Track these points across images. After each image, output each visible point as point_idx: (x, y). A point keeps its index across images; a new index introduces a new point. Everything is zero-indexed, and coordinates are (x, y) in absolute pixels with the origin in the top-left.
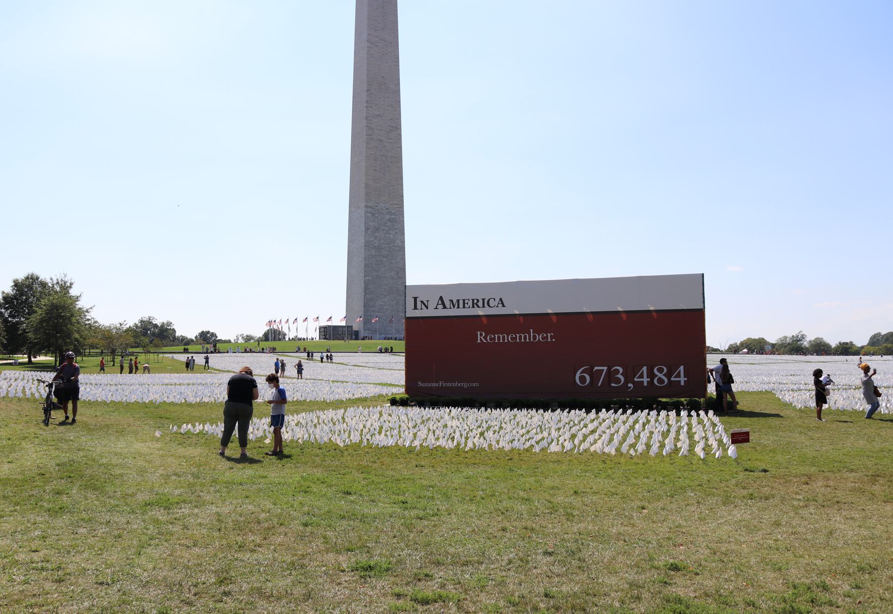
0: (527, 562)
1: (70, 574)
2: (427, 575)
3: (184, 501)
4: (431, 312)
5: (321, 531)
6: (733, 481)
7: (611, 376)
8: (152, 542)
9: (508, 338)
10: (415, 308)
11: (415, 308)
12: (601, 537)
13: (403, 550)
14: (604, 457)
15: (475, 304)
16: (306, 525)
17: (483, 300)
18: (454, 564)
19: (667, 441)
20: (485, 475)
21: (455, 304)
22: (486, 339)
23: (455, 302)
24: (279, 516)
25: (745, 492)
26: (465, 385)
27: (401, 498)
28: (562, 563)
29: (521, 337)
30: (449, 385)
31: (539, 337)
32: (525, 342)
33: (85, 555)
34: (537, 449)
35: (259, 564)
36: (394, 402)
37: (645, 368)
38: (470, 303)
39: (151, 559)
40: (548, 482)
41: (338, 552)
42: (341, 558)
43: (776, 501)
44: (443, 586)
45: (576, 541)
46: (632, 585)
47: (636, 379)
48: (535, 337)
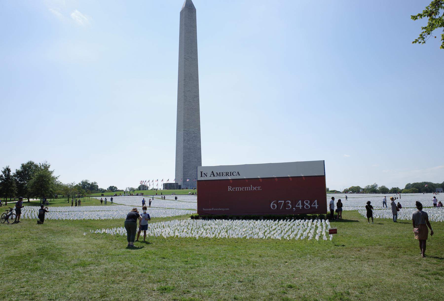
0: (231, 285)
1: (37, 296)
2: (188, 291)
3: (92, 264)
5: (149, 275)
6: (328, 250)
7: (286, 205)
8: (75, 281)
9: (242, 189)
10: (202, 176)
11: (202, 176)
12: (264, 275)
13: (181, 281)
14: (276, 241)
15: (227, 174)
16: (142, 272)
18: (201, 286)
19: (304, 233)
20: (224, 249)
24: (132, 269)
25: (331, 255)
26: (223, 210)
27: (186, 260)
28: (245, 285)
29: (247, 189)
30: (216, 209)
31: (255, 188)
33: (45, 288)
34: (248, 238)
35: (120, 289)
36: (192, 217)
37: (300, 201)
39: (74, 288)
40: (250, 252)
41: (154, 283)
42: (155, 285)
43: (343, 259)
44: (194, 296)
45: (253, 276)
46: (271, 294)
47: (296, 206)
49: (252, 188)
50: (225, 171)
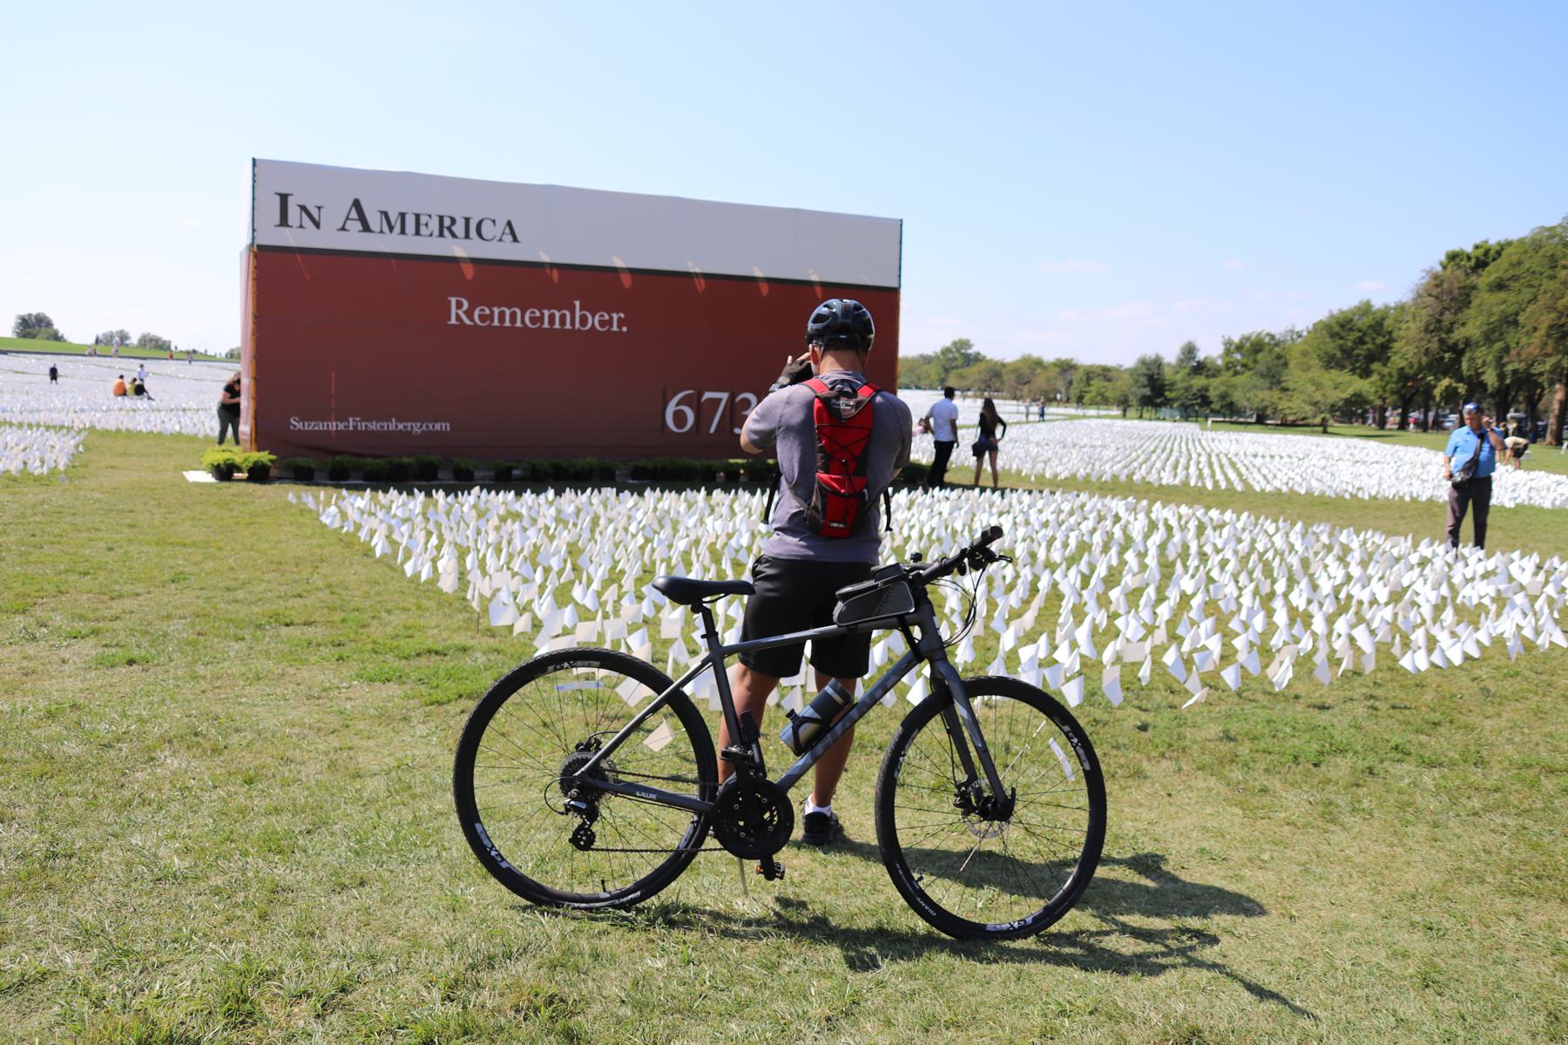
4: (327, 238)
9: (524, 319)
10: (284, 221)
11: (284, 221)
15: (445, 227)
17: (467, 220)
21: (396, 223)
22: (471, 318)
23: (393, 217)
26: (416, 428)
29: (553, 318)
30: (374, 426)
31: (594, 321)
32: (562, 331)
38: (434, 225)
48: (584, 320)
49: (577, 318)
50: (432, 207)
